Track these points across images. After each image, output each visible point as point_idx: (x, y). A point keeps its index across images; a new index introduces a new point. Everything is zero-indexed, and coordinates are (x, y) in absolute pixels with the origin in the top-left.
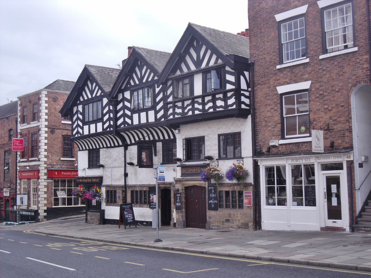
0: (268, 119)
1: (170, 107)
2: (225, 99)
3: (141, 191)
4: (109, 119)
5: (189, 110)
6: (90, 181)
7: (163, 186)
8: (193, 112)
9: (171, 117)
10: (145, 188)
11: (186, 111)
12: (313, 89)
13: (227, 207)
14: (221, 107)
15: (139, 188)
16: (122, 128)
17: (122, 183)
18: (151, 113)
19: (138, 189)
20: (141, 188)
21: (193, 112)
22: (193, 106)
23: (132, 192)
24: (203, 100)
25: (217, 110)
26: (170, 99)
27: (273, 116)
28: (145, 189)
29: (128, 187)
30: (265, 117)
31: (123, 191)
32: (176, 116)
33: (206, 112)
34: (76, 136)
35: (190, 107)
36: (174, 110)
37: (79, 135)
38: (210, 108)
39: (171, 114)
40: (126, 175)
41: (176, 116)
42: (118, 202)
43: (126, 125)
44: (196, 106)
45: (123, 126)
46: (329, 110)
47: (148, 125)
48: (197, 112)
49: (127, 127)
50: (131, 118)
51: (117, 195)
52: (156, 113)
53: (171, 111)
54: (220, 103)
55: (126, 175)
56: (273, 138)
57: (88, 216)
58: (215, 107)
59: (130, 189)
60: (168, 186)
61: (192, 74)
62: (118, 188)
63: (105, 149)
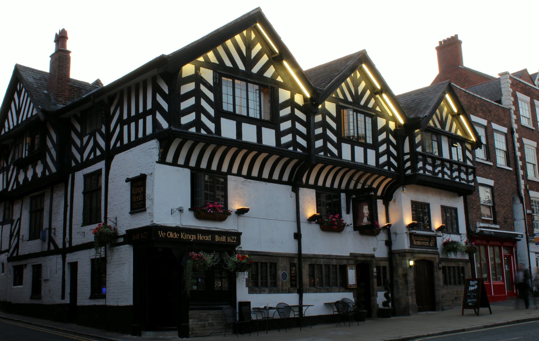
0: (474, 202)
1: (421, 160)
2: (467, 174)
3: (328, 266)
4: (293, 131)
5: (439, 171)
6: (208, 238)
7: (362, 259)
8: (443, 176)
9: (421, 172)
10: (334, 261)
11: (436, 171)
12: (495, 188)
13: (455, 283)
14: (463, 179)
15: (325, 260)
16: (320, 156)
17: (290, 248)
18: (371, 154)
19: (322, 262)
20: (328, 260)
21: (443, 176)
22: (443, 168)
23: (312, 266)
24: (451, 166)
25: (462, 181)
26: (419, 149)
27: (476, 201)
28: (334, 262)
29: (304, 258)
30: (472, 200)
31: (292, 265)
32: (427, 173)
33: (453, 180)
34: (193, 130)
35: (439, 168)
36: (424, 165)
37: (203, 132)
38: (456, 177)
39: (421, 168)
40: (298, 236)
41: (427, 173)
42: (282, 285)
43: (329, 155)
44: (446, 170)
45: (322, 153)
46: (504, 207)
47: (364, 168)
48: (446, 177)
49: (329, 158)
50: (338, 147)
51: (280, 273)
52: (378, 156)
53: (420, 164)
54: (463, 176)
55: (298, 236)
56: (478, 220)
57: (191, 320)
58: (459, 177)
59: (309, 263)
60: (369, 259)
61: (440, 132)
62: (280, 258)
63: (242, 179)
